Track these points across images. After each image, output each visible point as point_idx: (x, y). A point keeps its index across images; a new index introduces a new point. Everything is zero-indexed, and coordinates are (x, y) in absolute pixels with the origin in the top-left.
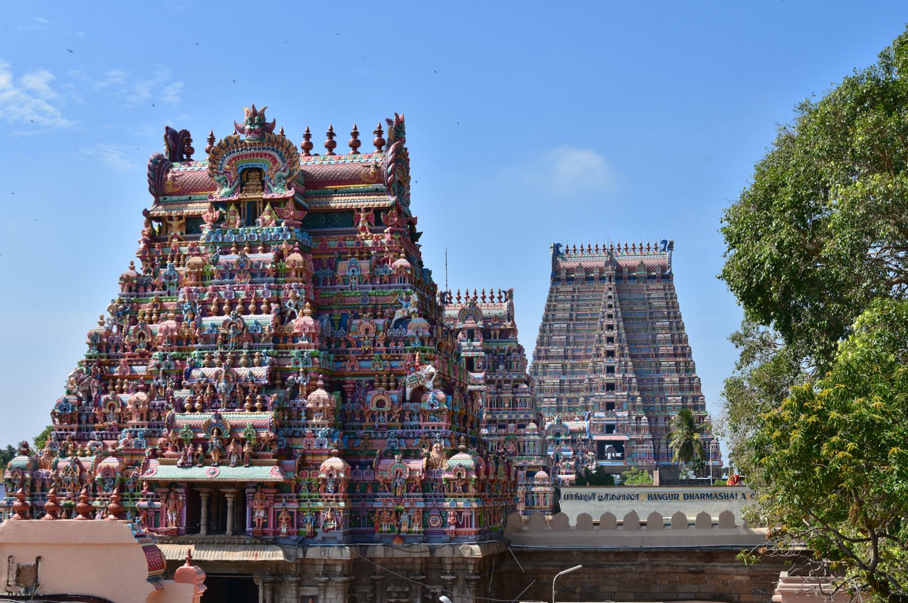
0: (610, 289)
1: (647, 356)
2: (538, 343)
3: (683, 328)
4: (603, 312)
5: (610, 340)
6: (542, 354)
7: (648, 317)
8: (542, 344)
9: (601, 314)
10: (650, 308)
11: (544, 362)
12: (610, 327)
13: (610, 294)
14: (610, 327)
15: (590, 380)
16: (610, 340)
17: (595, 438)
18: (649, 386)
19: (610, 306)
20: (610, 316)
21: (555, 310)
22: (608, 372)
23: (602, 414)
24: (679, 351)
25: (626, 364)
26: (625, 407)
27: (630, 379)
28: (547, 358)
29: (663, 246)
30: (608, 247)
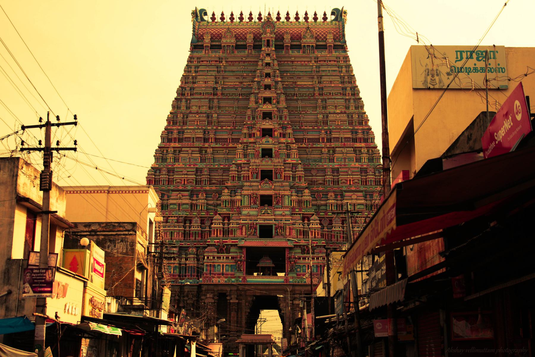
0: (268, 55)
1: (317, 140)
2: (168, 120)
3: (362, 107)
4: (258, 82)
5: (267, 115)
6: (175, 135)
7: (317, 93)
8: (175, 123)
9: (255, 85)
10: (320, 83)
11: (177, 145)
12: (267, 100)
13: (268, 60)
14: (267, 100)
15: (239, 165)
16: (267, 115)
17: (242, 243)
18: (320, 179)
19: (268, 75)
20: (268, 87)
21: (194, 83)
22: (263, 156)
23: (253, 212)
24: (360, 136)
25: (288, 146)
26: (287, 202)
27: (294, 166)
28: (180, 140)
29: (333, 17)
30: (264, 15)
